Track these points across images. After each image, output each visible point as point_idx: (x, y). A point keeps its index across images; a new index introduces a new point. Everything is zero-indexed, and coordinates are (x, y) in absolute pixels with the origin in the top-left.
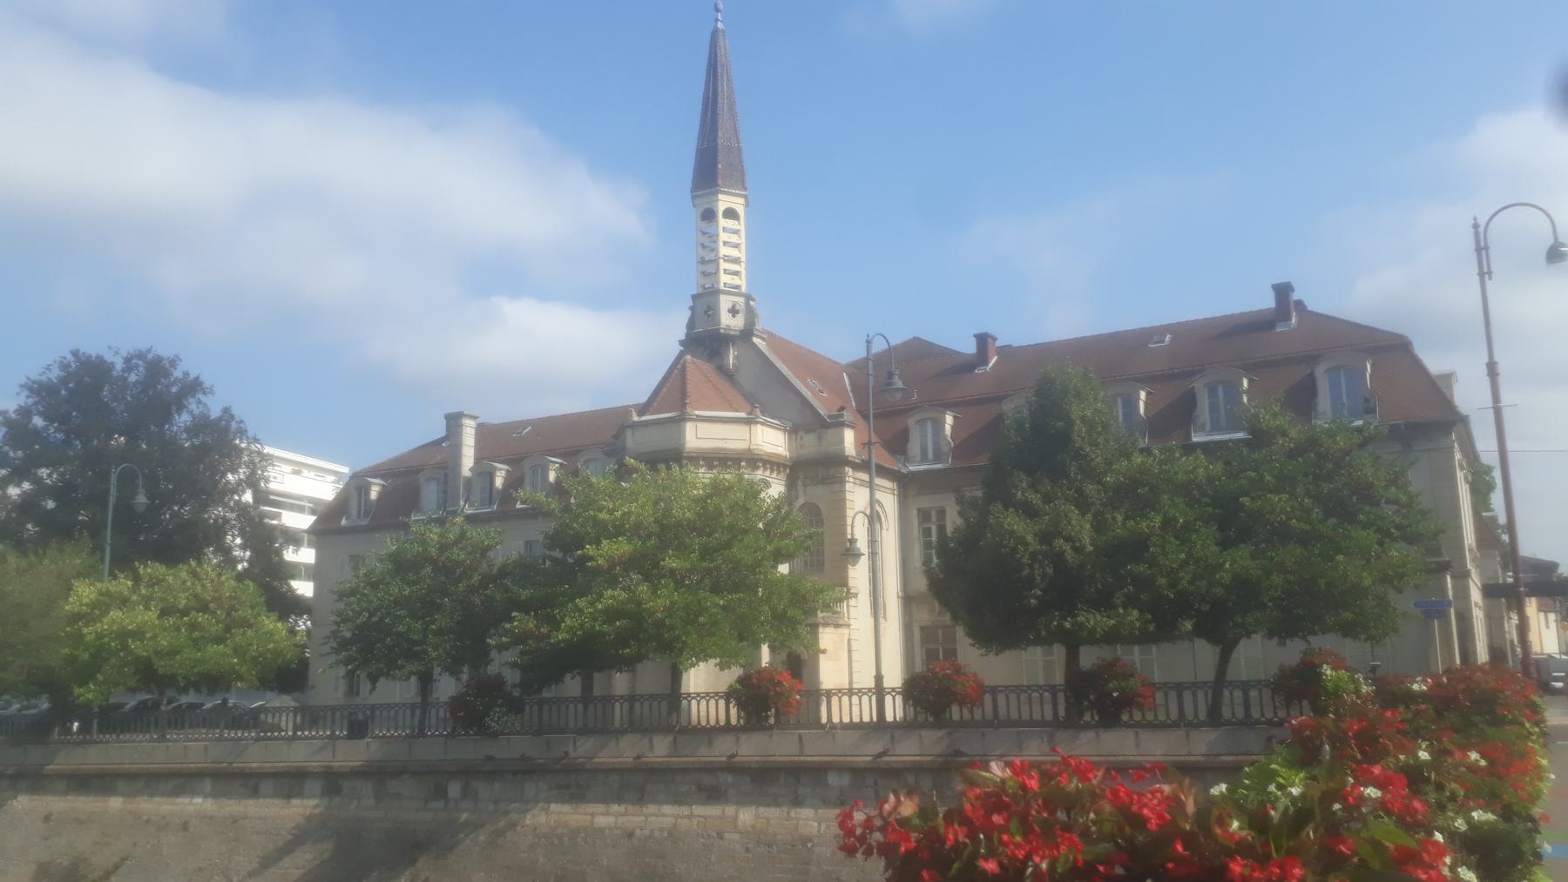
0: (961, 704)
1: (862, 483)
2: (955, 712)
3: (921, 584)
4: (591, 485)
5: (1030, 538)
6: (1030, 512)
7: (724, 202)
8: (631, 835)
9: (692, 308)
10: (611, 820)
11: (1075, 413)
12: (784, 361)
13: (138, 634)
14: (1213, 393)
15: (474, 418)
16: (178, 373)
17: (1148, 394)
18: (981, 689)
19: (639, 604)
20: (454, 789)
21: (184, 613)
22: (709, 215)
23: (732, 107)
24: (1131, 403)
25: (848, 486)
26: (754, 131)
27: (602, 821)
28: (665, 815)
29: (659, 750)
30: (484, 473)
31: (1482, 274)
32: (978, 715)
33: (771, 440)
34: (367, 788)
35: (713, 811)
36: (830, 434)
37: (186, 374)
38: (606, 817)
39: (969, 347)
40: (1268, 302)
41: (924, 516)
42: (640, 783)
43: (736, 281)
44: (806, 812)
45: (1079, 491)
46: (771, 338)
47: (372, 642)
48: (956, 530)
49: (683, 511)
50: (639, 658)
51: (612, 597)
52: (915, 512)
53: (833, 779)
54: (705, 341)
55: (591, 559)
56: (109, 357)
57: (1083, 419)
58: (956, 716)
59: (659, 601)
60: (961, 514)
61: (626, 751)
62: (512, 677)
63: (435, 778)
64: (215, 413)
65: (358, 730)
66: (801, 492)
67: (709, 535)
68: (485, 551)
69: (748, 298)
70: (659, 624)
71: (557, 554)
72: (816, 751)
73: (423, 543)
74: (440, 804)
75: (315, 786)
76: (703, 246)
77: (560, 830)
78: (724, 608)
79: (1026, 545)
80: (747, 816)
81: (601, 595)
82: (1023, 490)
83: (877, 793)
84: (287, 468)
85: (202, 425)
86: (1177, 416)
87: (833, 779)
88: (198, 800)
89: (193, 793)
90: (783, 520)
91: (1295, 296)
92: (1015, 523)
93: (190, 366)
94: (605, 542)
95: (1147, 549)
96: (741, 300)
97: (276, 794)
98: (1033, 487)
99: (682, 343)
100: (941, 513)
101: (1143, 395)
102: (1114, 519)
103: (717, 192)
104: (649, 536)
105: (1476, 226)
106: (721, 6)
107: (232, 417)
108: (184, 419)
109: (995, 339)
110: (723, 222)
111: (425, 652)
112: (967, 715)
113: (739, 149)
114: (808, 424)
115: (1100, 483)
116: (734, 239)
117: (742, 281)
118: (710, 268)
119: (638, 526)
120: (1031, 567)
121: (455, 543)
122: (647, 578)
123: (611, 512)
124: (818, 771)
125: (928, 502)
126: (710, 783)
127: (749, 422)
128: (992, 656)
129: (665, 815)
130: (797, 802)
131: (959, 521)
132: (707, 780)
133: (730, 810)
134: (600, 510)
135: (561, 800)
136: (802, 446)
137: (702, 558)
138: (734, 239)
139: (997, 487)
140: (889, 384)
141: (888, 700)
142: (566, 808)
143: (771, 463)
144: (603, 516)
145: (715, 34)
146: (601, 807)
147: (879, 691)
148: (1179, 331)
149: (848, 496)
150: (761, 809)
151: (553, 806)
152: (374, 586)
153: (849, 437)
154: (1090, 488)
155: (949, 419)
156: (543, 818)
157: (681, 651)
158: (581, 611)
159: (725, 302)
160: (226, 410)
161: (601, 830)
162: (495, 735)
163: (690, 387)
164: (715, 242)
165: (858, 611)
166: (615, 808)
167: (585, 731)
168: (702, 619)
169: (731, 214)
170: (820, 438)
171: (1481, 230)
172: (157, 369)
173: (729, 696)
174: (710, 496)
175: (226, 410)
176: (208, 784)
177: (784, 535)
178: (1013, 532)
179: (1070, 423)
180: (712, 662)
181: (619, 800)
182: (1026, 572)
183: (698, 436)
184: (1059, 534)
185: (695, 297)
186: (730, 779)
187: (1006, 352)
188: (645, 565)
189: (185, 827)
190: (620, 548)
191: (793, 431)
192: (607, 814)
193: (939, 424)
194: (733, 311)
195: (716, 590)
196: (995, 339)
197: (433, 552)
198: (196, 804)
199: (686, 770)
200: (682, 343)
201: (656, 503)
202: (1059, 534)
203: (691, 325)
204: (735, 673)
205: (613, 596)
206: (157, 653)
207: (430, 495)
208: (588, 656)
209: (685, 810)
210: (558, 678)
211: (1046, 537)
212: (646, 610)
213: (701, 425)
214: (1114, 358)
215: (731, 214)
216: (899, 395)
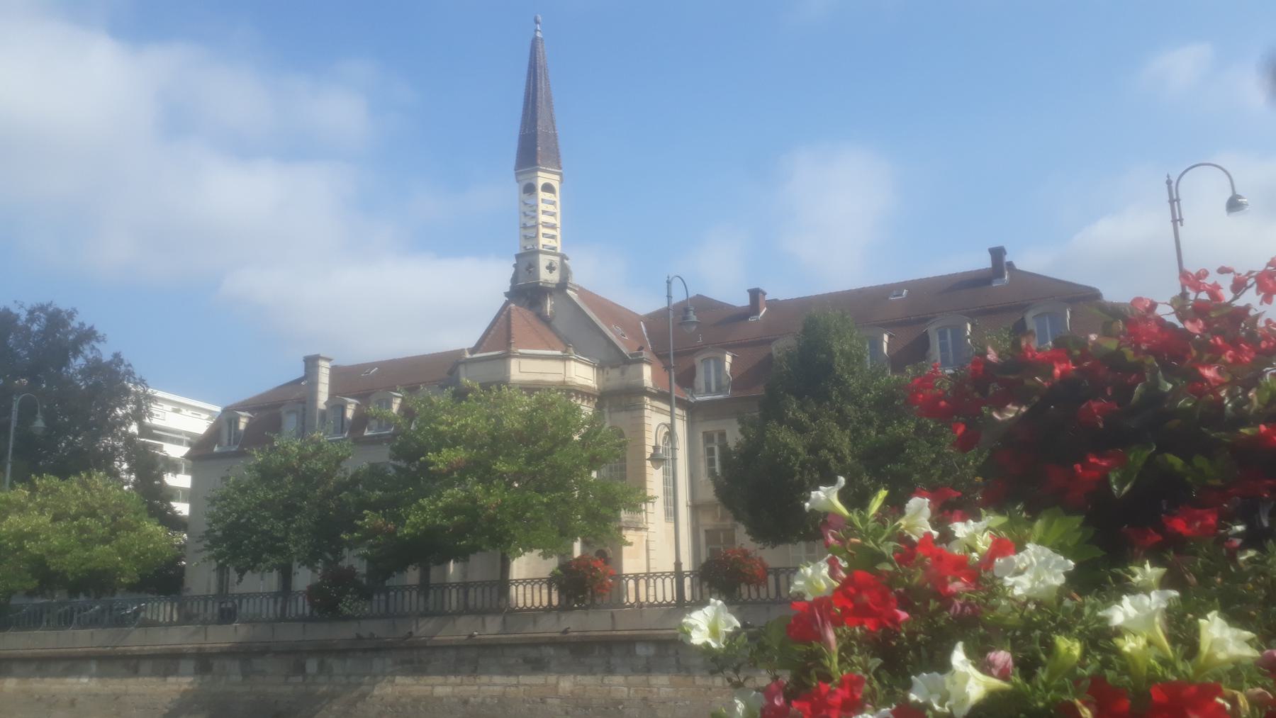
0: (748, 584)
1: (659, 411)
2: (744, 589)
3: (709, 494)
4: (431, 404)
5: (800, 450)
6: (800, 428)
7: (542, 178)
8: (466, 702)
9: (515, 266)
10: (448, 690)
11: (836, 347)
12: (593, 310)
13: (33, 536)
14: (943, 336)
15: (329, 360)
16: (75, 324)
17: (890, 337)
18: (766, 571)
19: (474, 501)
20: (312, 665)
21: (75, 518)
22: (530, 189)
23: (549, 101)
24: (876, 344)
25: (647, 413)
26: (568, 119)
27: (440, 691)
28: (495, 685)
29: (491, 628)
30: (337, 407)
31: (1174, 221)
32: (763, 595)
33: (582, 374)
34: (234, 666)
35: (537, 679)
36: (631, 369)
37: (82, 324)
38: (443, 687)
39: (743, 301)
40: (985, 262)
41: (708, 438)
42: (473, 656)
43: (552, 243)
44: (617, 679)
45: (840, 411)
46: (582, 292)
47: (239, 538)
48: (738, 444)
49: (512, 423)
50: (475, 549)
51: (452, 496)
52: (701, 435)
53: (641, 650)
54: (527, 291)
55: (432, 464)
56: (15, 310)
57: (842, 352)
58: (745, 596)
59: (491, 499)
60: (742, 431)
61: (462, 629)
62: (361, 567)
63: (294, 656)
64: (107, 357)
65: (227, 616)
66: (607, 416)
67: (534, 443)
68: (339, 460)
69: (563, 257)
70: (492, 520)
71: (402, 464)
72: (625, 627)
73: (286, 454)
74: (300, 679)
75: (188, 665)
76: (525, 215)
77: (403, 700)
78: (547, 505)
79: (797, 455)
80: (566, 684)
81: (440, 496)
82: (792, 409)
83: (678, 661)
84: (168, 407)
85: (96, 367)
86: (916, 351)
87: (641, 650)
88: (85, 680)
89: (79, 674)
90: (596, 434)
91: (1007, 259)
92: (787, 437)
93: (85, 317)
94: (444, 450)
95: (903, 451)
96: (557, 259)
97: (154, 673)
98: (801, 408)
99: (507, 294)
100: (722, 435)
101: (886, 337)
102: (868, 434)
103: (537, 170)
104: (481, 447)
105: (1169, 183)
106: (540, 18)
107: (122, 361)
108: (78, 363)
109: (764, 294)
110: (542, 195)
111: (287, 547)
112: (754, 595)
113: (555, 135)
114: (611, 359)
115: (856, 404)
116: (551, 208)
117: (557, 244)
118: (530, 233)
119: (474, 436)
120: (801, 473)
121: (314, 454)
122: (481, 480)
123: (451, 424)
124: (629, 643)
125: (711, 426)
126: (533, 654)
127: (564, 359)
128: (768, 549)
129: (495, 685)
130: (610, 671)
131: (741, 437)
132: (533, 653)
133: (552, 679)
134: (441, 424)
135: (407, 675)
136: (608, 380)
137: (528, 463)
138: (551, 208)
139: (771, 409)
140: (685, 318)
141: (687, 581)
142: (408, 680)
143: (584, 393)
144: (443, 428)
145: (535, 41)
146: (439, 679)
147: (678, 574)
148: (918, 288)
149: (647, 421)
150: (579, 678)
151: (399, 679)
152: (243, 491)
153: (647, 371)
154: (849, 408)
155: (728, 358)
156: (389, 689)
157: (510, 543)
158: (422, 508)
159: (543, 261)
160: (117, 356)
161: (440, 699)
162: (347, 618)
163: (514, 331)
164: (535, 211)
165: (655, 514)
166: (452, 679)
167: (427, 614)
168: (528, 515)
169: (548, 188)
170: (623, 373)
171: (1174, 185)
172: (56, 320)
173: (551, 581)
174: (535, 410)
175: (117, 356)
176: (93, 666)
177: (600, 443)
178: (786, 445)
179: (831, 354)
180: (536, 552)
181: (456, 672)
182: (797, 477)
183: (522, 370)
184: (824, 446)
185: (518, 257)
186: (551, 651)
187: (774, 305)
188: (481, 470)
189: (73, 703)
190: (459, 455)
191: (600, 367)
192: (444, 684)
193: (720, 362)
194: (551, 268)
195: (540, 490)
196: (764, 294)
197: (295, 462)
198: (82, 684)
199: (513, 645)
200: (507, 294)
201: (488, 419)
202: (824, 446)
203: (515, 279)
204: (553, 563)
205: (452, 494)
206: (50, 552)
207: (290, 424)
208: (429, 548)
209: (513, 680)
210: (402, 568)
211: (813, 450)
212: (482, 507)
213: (524, 362)
214: (865, 307)
215: (548, 188)
216: (694, 328)
